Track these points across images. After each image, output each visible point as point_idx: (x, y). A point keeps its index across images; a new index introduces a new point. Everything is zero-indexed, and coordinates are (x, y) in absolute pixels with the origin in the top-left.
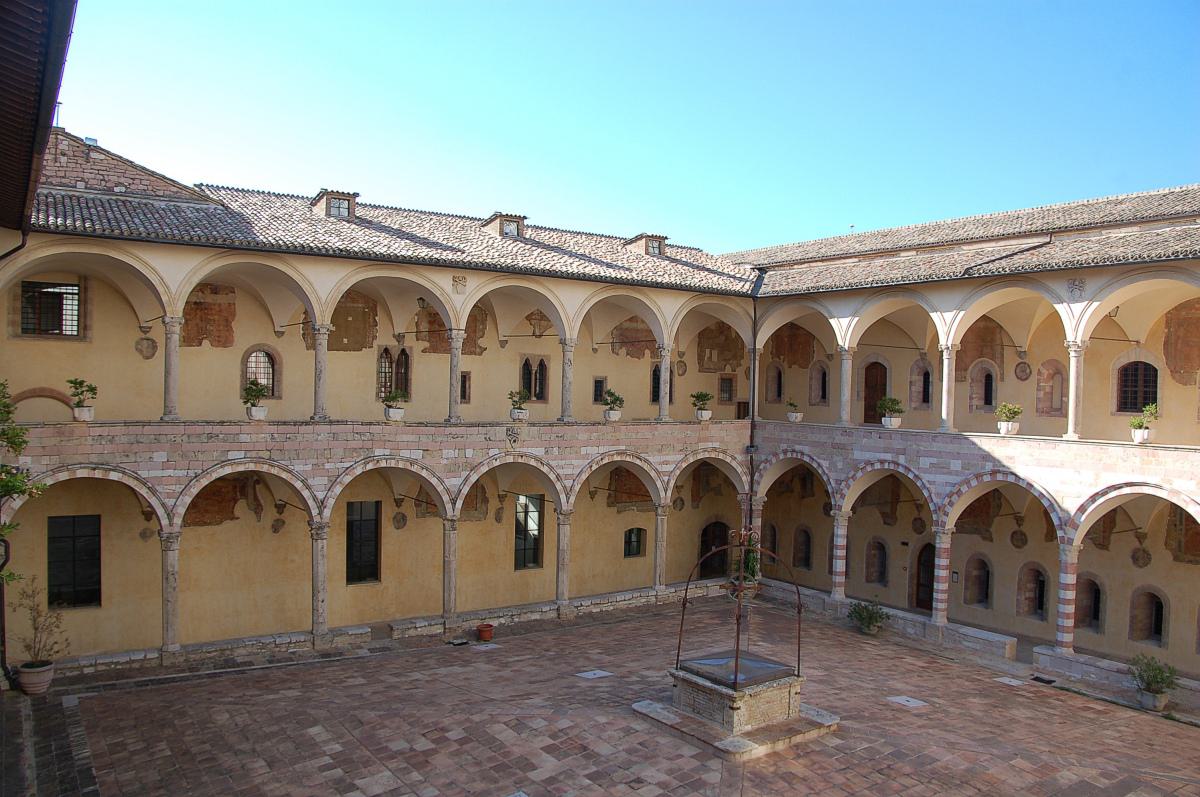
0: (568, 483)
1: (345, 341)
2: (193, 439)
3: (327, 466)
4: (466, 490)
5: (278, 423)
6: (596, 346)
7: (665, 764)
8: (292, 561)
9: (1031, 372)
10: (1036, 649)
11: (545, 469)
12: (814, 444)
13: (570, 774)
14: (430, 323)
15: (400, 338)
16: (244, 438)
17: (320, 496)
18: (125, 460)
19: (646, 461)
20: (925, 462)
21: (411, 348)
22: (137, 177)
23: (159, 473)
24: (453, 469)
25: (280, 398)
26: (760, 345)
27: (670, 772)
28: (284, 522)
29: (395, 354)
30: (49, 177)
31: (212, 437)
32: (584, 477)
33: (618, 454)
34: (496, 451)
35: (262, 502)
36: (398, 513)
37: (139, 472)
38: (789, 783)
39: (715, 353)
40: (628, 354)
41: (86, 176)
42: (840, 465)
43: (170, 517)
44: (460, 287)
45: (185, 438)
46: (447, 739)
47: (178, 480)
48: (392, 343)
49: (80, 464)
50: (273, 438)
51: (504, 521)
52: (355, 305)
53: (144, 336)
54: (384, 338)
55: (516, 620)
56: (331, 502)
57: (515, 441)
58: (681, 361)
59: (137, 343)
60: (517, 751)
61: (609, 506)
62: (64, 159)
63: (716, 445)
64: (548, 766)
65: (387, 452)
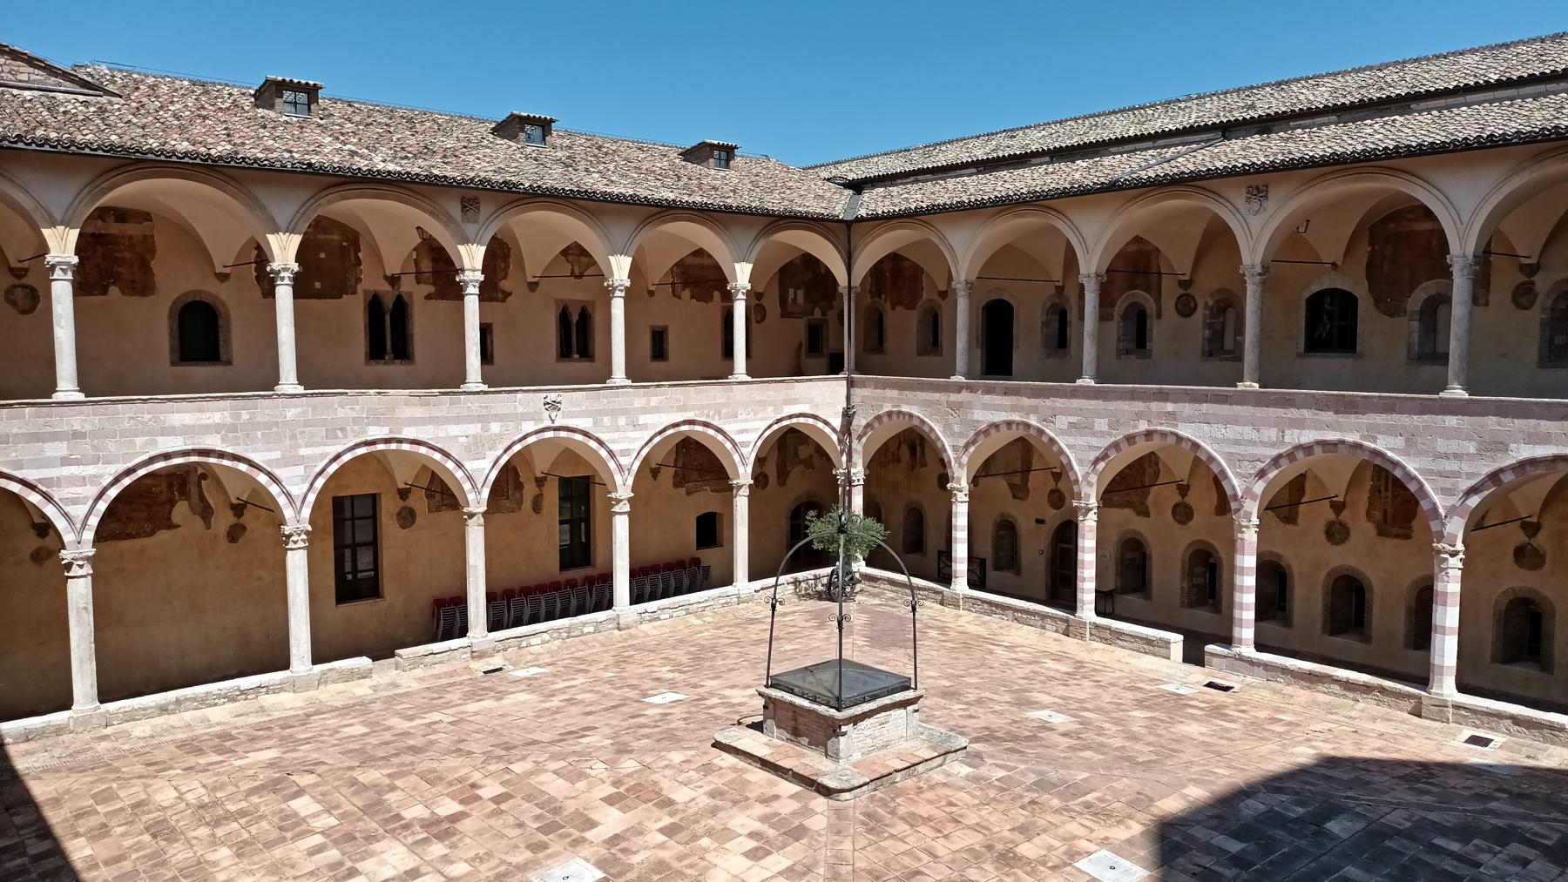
1: (318, 285)
3: (303, 451)
6: (653, 288)
7: (760, 809)
9: (1196, 306)
10: (1210, 648)
11: (593, 444)
12: (926, 404)
13: (638, 831)
15: (394, 280)
19: (719, 430)
20: (1062, 421)
21: (410, 294)
24: (477, 447)
25: (229, 363)
26: (856, 282)
27: (764, 819)
28: (244, 528)
29: (389, 302)
35: (211, 502)
38: (912, 826)
39: (800, 293)
40: (692, 297)
42: (956, 428)
44: (470, 214)
46: (479, 798)
48: (385, 287)
51: (544, 511)
52: (329, 237)
53: (17, 282)
54: (371, 281)
58: (757, 305)
60: (571, 806)
61: (676, 485)
63: (806, 409)
64: (612, 821)
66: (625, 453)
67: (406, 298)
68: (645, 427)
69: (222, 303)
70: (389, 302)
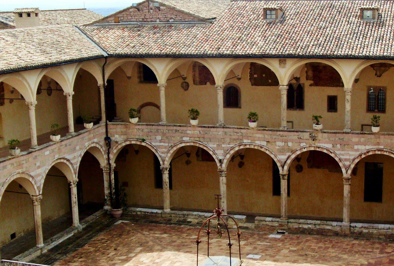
0: (347, 163)
1: (270, 81)
2: (170, 132)
3: (223, 146)
4: (289, 161)
5: (201, 127)
8: (248, 181)
11: (332, 155)
14: (314, 71)
16: (189, 132)
17: (221, 158)
18: (147, 138)
21: (304, 84)
22: (178, 14)
23: (158, 144)
24: (282, 151)
25: (240, 108)
29: (295, 87)
30: (147, 19)
31: (176, 131)
32: (357, 161)
33: (379, 150)
34: (304, 144)
36: (299, 165)
37: (152, 143)
41: (160, 16)
43: (163, 161)
44: (282, 65)
45: (167, 131)
47: (165, 147)
49: (133, 138)
50: (200, 133)
53: (184, 81)
55: (318, 227)
56: (225, 161)
57: (314, 140)
59: (182, 84)
62: (151, 11)
65: (249, 141)
66: (346, 160)
67: (302, 85)
68: (357, 150)
69: (239, 87)
70: (295, 87)
